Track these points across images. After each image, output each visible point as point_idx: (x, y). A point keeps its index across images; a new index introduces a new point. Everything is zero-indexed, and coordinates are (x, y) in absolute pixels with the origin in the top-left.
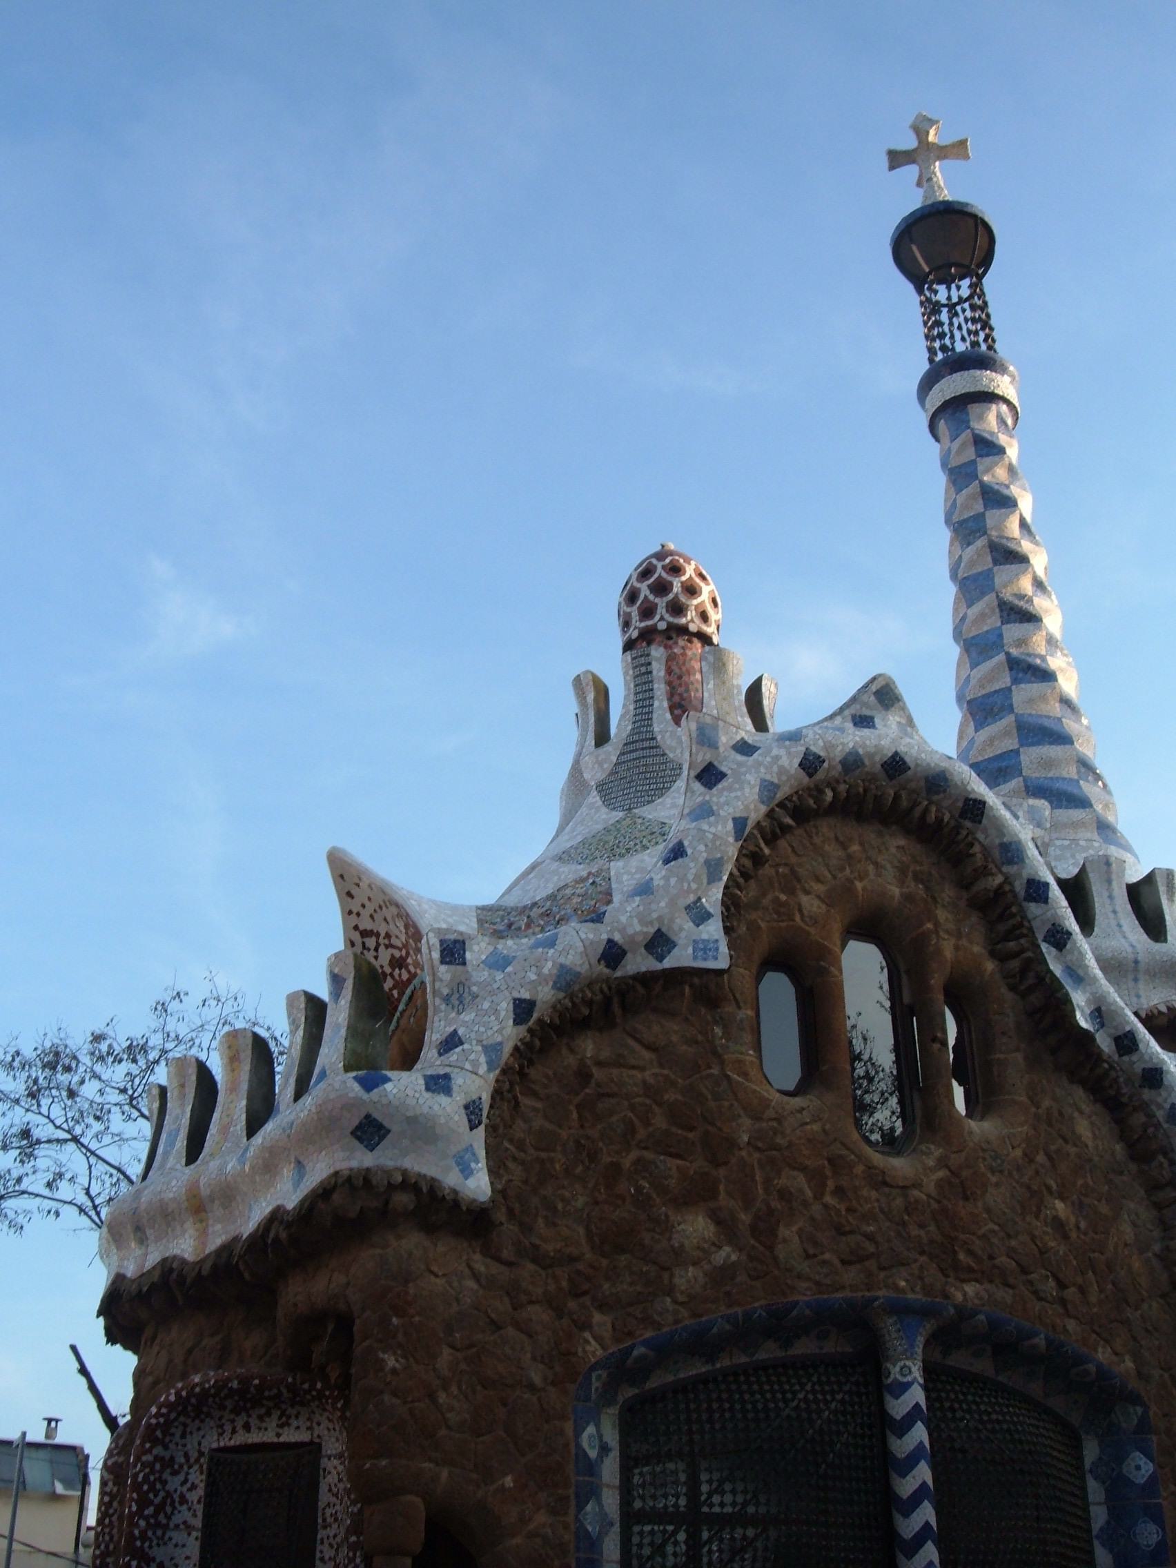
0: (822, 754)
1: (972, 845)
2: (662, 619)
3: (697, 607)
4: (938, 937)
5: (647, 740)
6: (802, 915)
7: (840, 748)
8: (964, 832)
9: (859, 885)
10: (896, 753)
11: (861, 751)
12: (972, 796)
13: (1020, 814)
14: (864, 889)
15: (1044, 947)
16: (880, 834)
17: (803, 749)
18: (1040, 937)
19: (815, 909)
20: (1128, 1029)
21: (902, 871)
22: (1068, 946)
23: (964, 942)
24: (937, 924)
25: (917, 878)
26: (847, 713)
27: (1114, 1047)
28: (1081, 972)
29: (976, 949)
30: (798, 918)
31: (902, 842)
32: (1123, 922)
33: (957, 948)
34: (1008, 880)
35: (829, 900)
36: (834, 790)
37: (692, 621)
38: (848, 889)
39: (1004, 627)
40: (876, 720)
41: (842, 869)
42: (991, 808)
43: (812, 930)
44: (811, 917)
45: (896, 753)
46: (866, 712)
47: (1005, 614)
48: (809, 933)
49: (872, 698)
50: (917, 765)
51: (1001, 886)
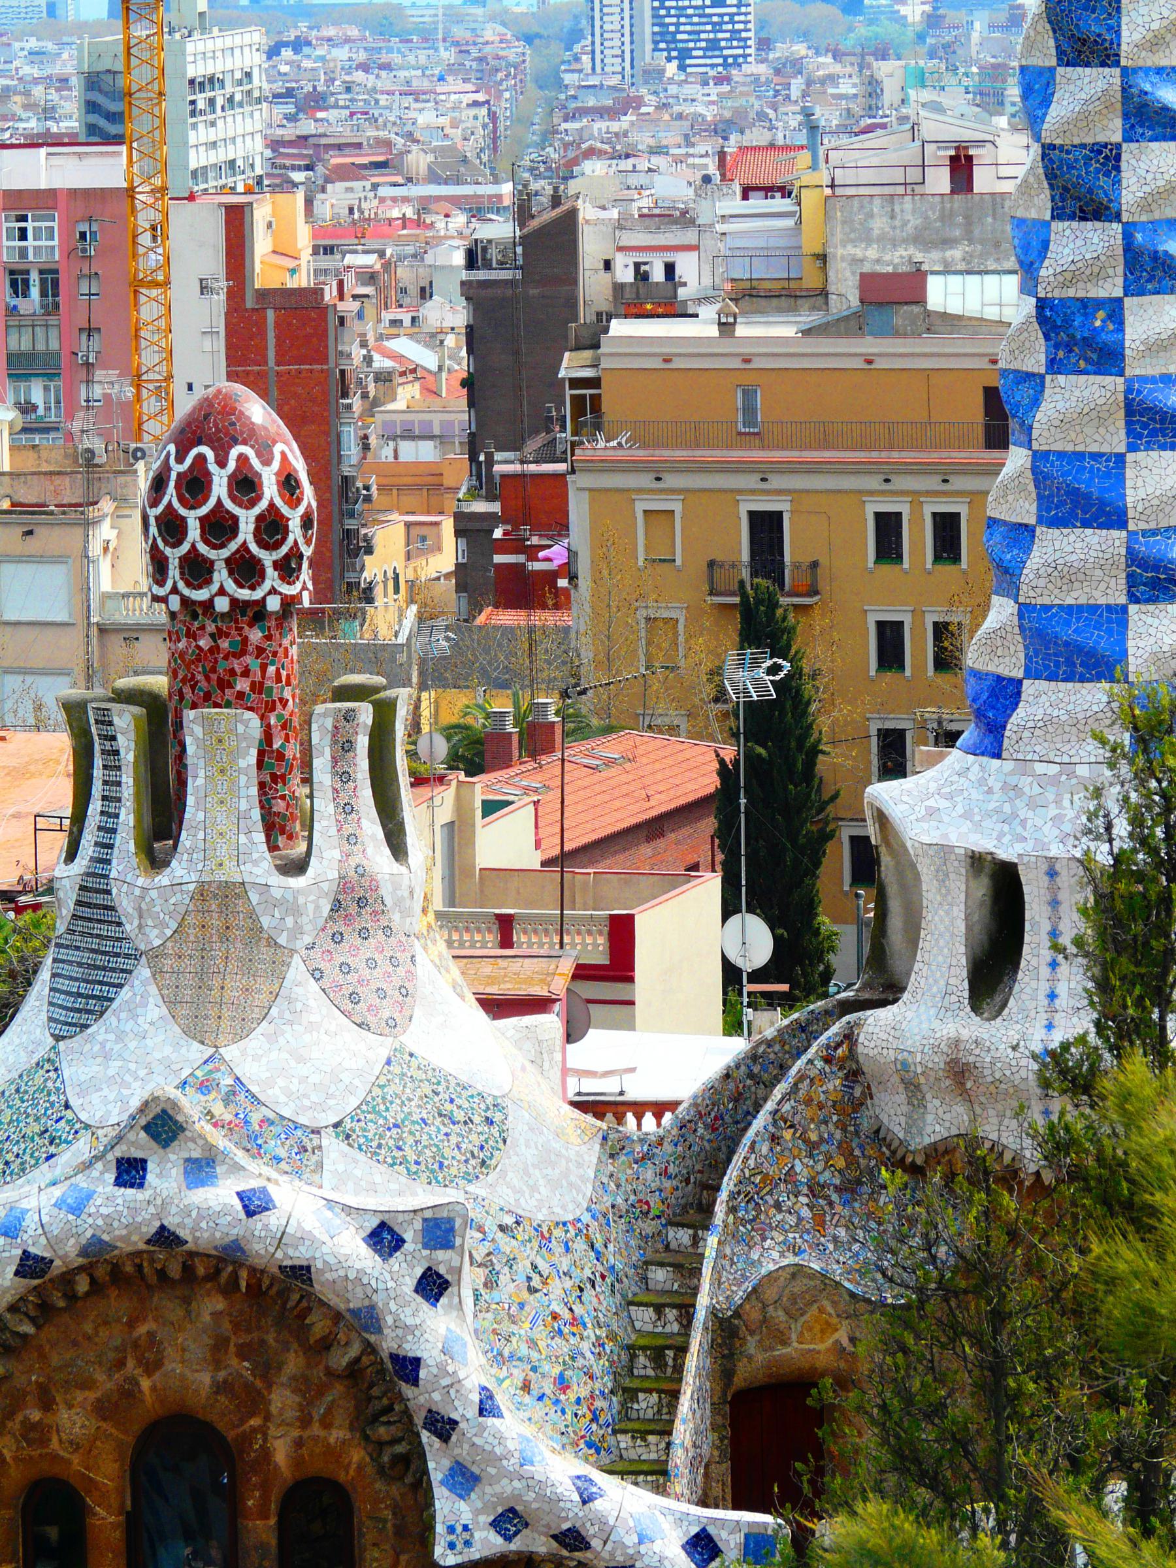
0: (46, 1255)
1: (309, 1309)
2: (175, 590)
3: (228, 561)
4: (265, 1435)
5: (98, 891)
6: (60, 1441)
7: (72, 1241)
8: (296, 1297)
9: (145, 1384)
10: (163, 1227)
11: (106, 1237)
12: (288, 1263)
13: (408, 1236)
14: (153, 1388)
15: (425, 1436)
16: (187, 1301)
17: (20, 1252)
18: (419, 1420)
19: (76, 1430)
20: (565, 1526)
21: (219, 1345)
22: (454, 1438)
23: (316, 1429)
24: (267, 1418)
25: (244, 1353)
26: (110, 1157)
27: (555, 1544)
28: (475, 1469)
29: (337, 1435)
30: (54, 1443)
31: (219, 1304)
32: (1062, 989)
33: (299, 1443)
34: (370, 1349)
35: (102, 1410)
36: (91, 1277)
37: (222, 592)
38: (129, 1393)
39: (1058, 226)
40: (150, 1166)
41: (121, 1364)
42: (322, 1272)
43: (76, 1459)
44: (71, 1442)
45: (163, 1227)
46: (139, 1154)
47: (1058, 193)
48: (69, 1462)
49: (143, 1134)
50: (196, 1239)
51: (357, 1360)
